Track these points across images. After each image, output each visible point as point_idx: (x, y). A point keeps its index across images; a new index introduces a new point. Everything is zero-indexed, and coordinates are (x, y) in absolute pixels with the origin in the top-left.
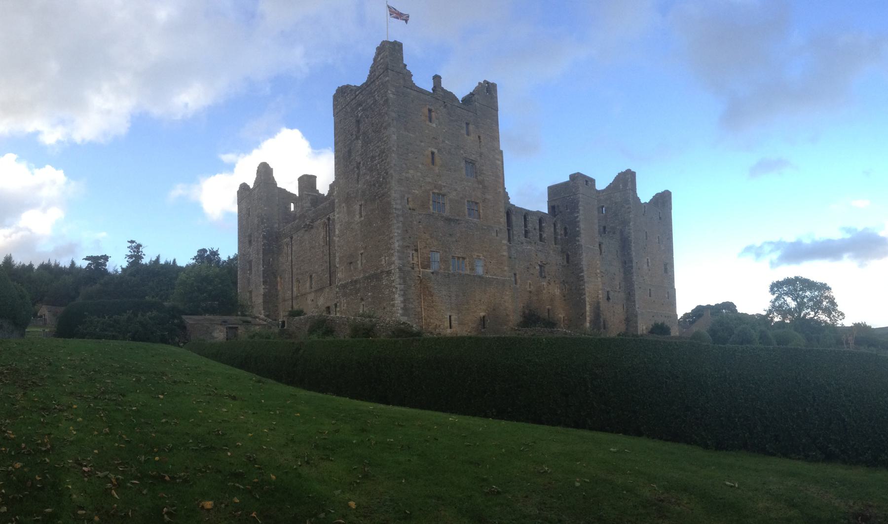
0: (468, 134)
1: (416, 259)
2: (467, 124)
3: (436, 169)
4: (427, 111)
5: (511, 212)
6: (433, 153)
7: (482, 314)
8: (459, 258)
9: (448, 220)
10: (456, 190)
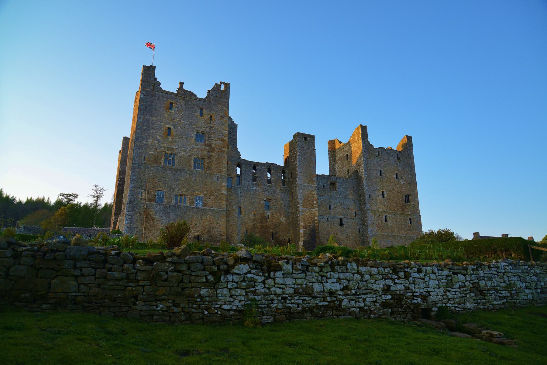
0: (201, 115)
1: (144, 195)
2: (201, 109)
3: (171, 139)
4: (168, 103)
8: (181, 195)
9: (176, 170)
10: (185, 151)
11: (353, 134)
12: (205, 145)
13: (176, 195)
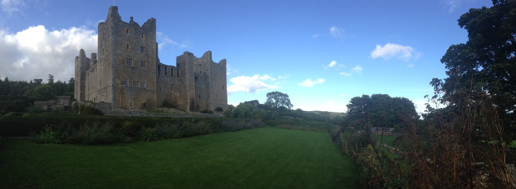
5: (160, 66)
6: (128, 44)
7: (144, 102)
9: (133, 68)
11: (205, 54)
12: (146, 54)
13: (134, 81)
